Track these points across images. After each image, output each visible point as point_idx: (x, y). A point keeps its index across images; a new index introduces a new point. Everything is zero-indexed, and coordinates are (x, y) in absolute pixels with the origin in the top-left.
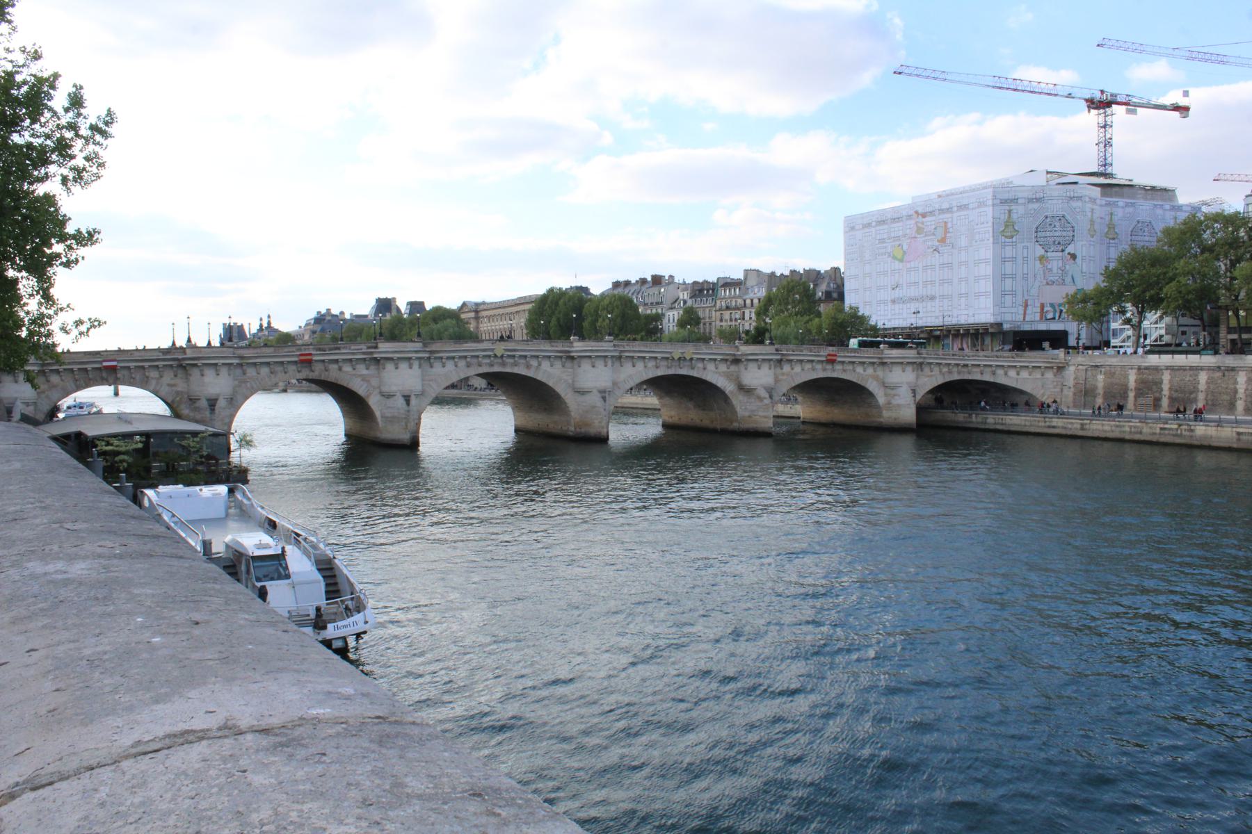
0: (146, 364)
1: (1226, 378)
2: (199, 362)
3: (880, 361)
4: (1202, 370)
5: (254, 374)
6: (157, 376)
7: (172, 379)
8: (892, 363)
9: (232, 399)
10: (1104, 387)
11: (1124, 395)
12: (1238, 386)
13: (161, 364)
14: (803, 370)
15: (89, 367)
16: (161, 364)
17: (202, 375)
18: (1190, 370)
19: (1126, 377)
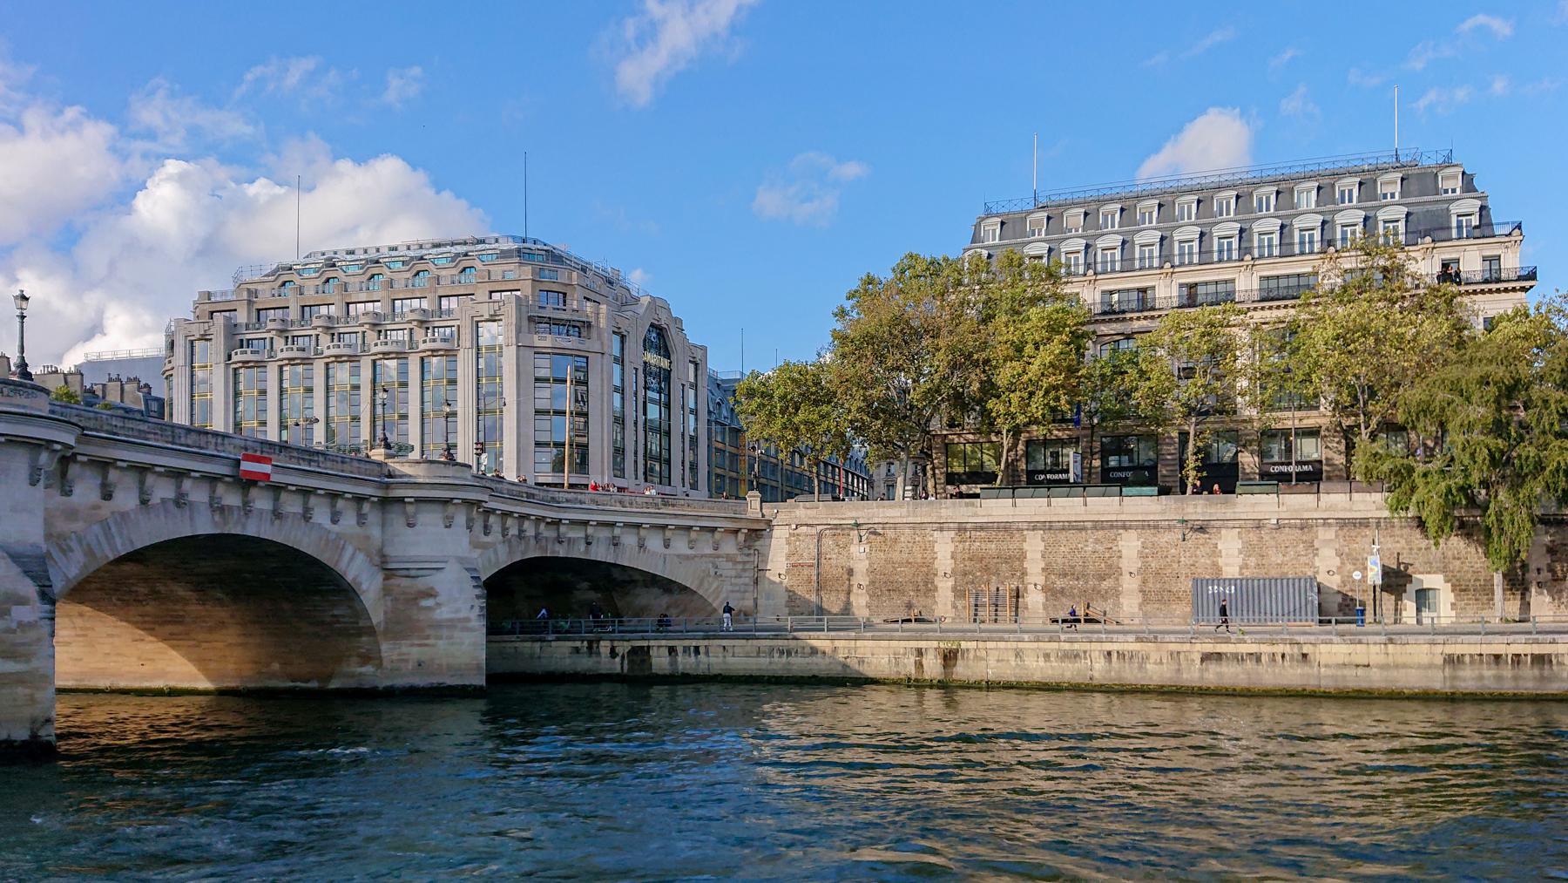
1: (1189, 544)
3: (380, 493)
4: (1125, 528)
8: (419, 500)
10: (871, 571)
11: (927, 586)
12: (1221, 561)
14: (144, 502)
18: (1095, 528)
19: (929, 547)
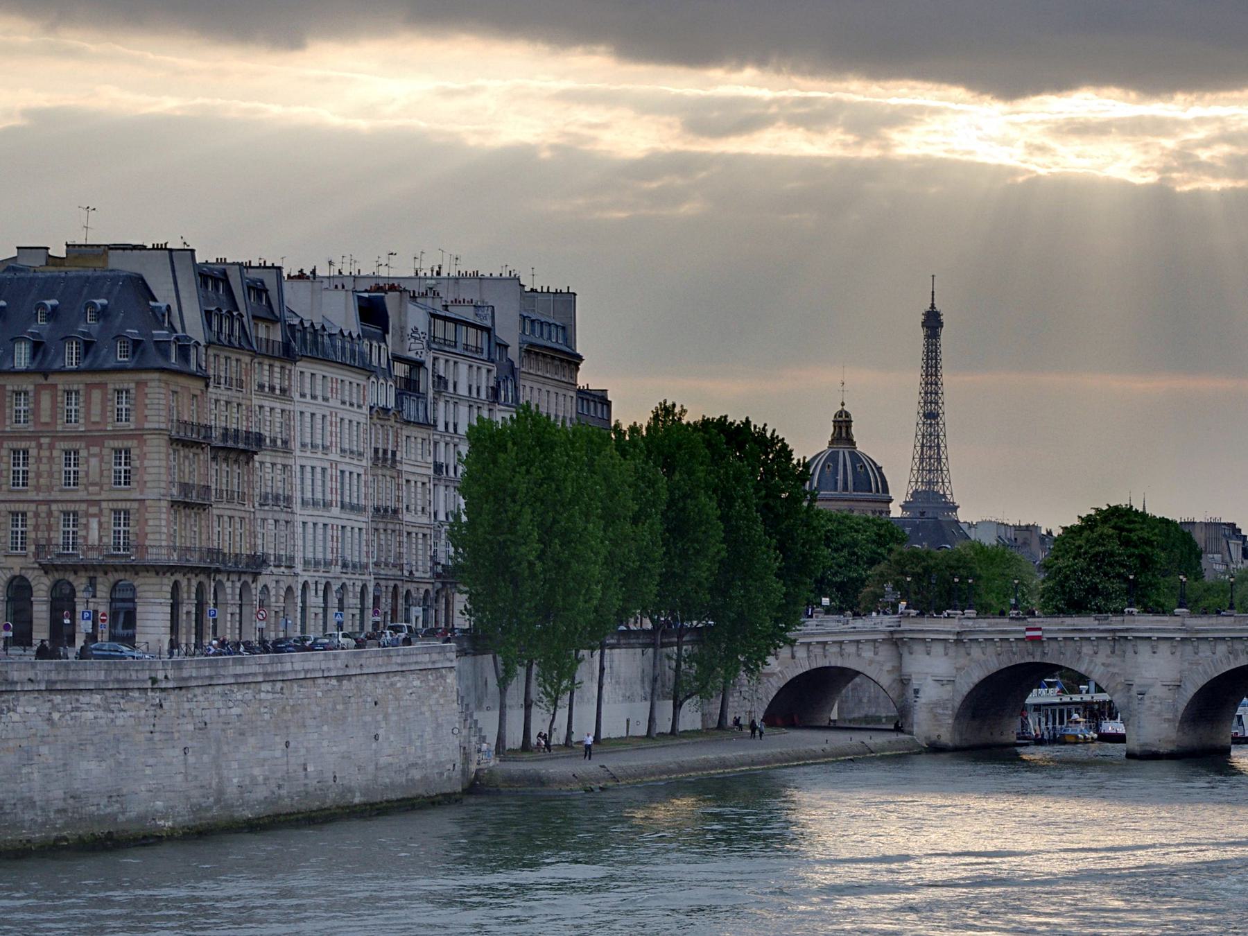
0: (1077, 636)
2: (1130, 635)
5: (1209, 653)
6: (1091, 652)
7: (1108, 656)
9: (1179, 686)
13: (1093, 636)
15: (1012, 637)
16: (1093, 636)
17: (1136, 653)
